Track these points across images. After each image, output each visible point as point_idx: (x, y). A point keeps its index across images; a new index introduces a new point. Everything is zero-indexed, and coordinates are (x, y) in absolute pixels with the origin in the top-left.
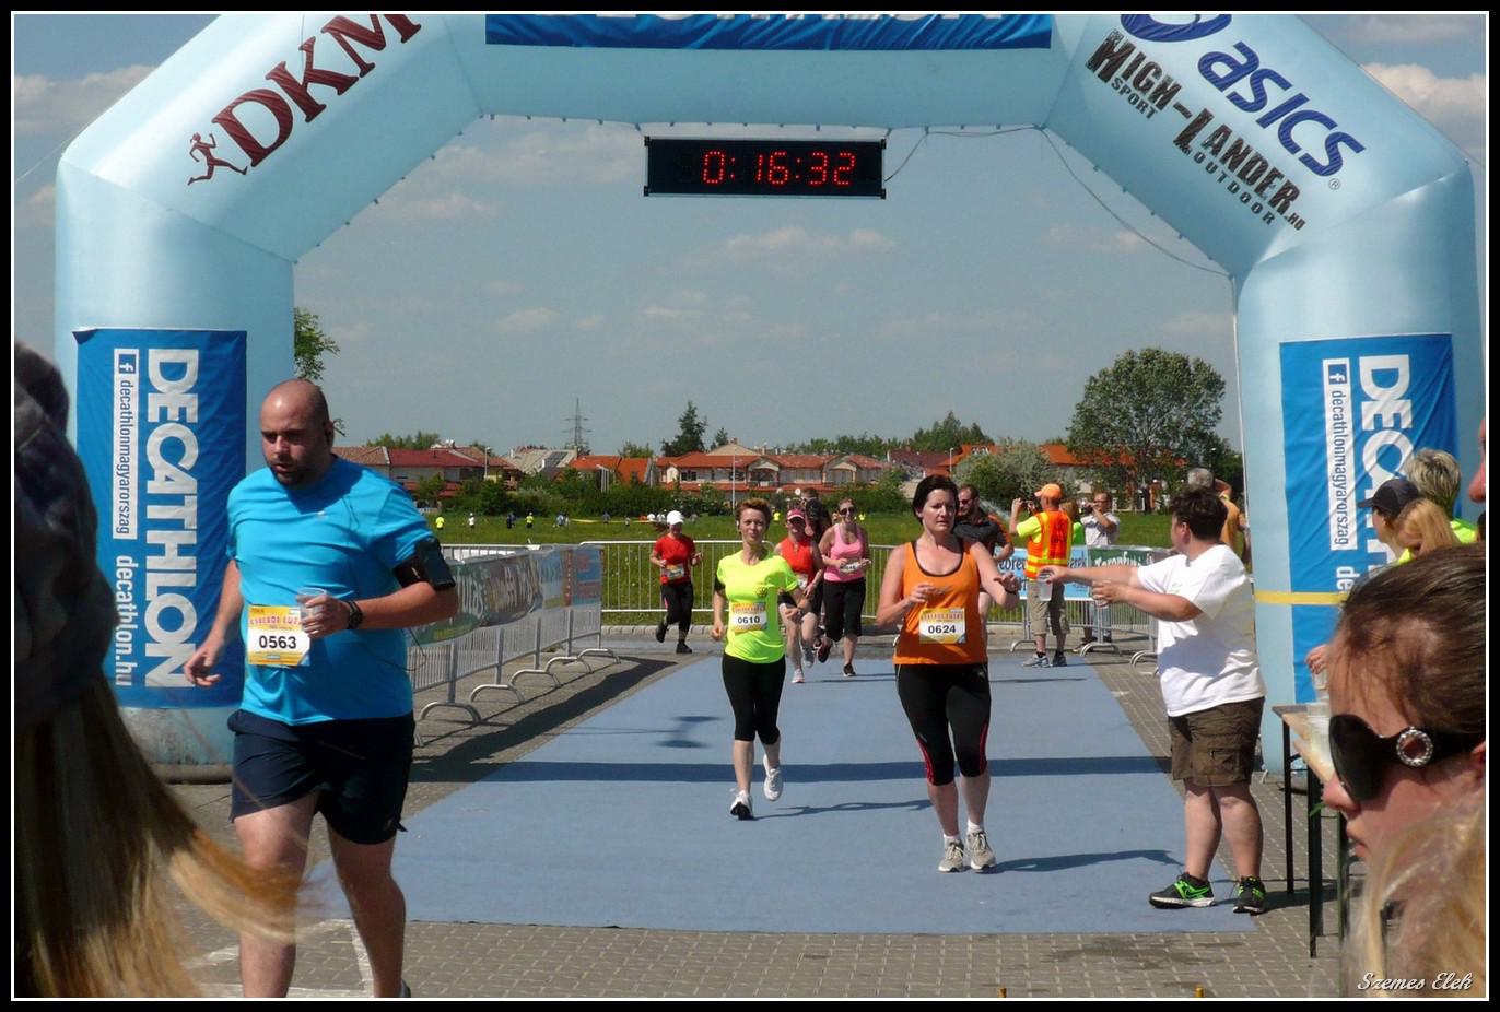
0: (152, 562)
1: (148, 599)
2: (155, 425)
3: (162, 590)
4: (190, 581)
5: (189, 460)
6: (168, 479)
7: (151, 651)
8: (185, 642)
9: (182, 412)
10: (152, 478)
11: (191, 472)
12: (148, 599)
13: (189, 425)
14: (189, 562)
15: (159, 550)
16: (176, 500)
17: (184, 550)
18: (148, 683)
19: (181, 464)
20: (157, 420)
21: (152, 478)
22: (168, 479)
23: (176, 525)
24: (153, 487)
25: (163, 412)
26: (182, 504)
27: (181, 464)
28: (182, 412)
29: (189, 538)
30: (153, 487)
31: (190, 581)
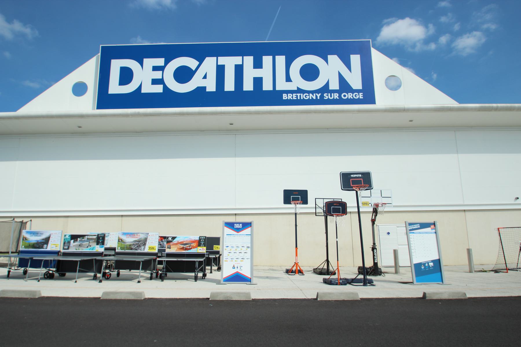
0: (267, 86)
1: (296, 89)
2: (165, 88)
3: (288, 79)
4: (281, 60)
5: (191, 63)
6: (205, 77)
7: (334, 85)
8: (326, 61)
9: (155, 69)
10: (205, 88)
11: (201, 61)
12: (296, 89)
13: (166, 63)
14: (267, 60)
15: (258, 82)
16: (221, 70)
17: (258, 64)
18: (361, 88)
19: (194, 69)
20: (162, 86)
21: (205, 88)
22: (205, 77)
23: (239, 70)
24: (211, 86)
25: (155, 82)
26: (223, 66)
27: (194, 69)
28: (155, 69)
29: (249, 61)
30: (211, 86)
31: (281, 60)
